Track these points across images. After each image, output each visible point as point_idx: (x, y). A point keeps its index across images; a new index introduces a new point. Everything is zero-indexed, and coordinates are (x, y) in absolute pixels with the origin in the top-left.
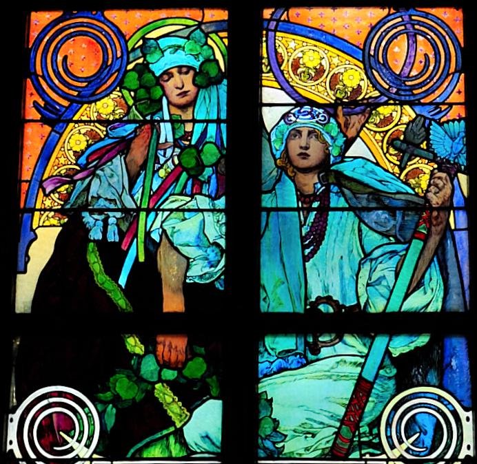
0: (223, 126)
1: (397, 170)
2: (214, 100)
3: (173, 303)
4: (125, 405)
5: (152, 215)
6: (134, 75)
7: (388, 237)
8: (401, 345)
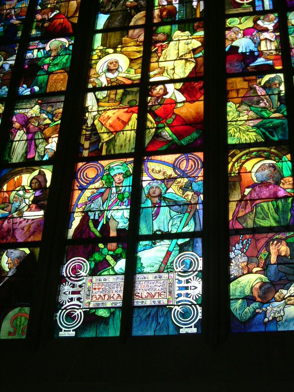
0: (131, 187)
1: (182, 195)
2: (128, 181)
3: (113, 234)
4: (97, 261)
5: (109, 211)
6: (106, 176)
7: (178, 213)
8: (181, 241)
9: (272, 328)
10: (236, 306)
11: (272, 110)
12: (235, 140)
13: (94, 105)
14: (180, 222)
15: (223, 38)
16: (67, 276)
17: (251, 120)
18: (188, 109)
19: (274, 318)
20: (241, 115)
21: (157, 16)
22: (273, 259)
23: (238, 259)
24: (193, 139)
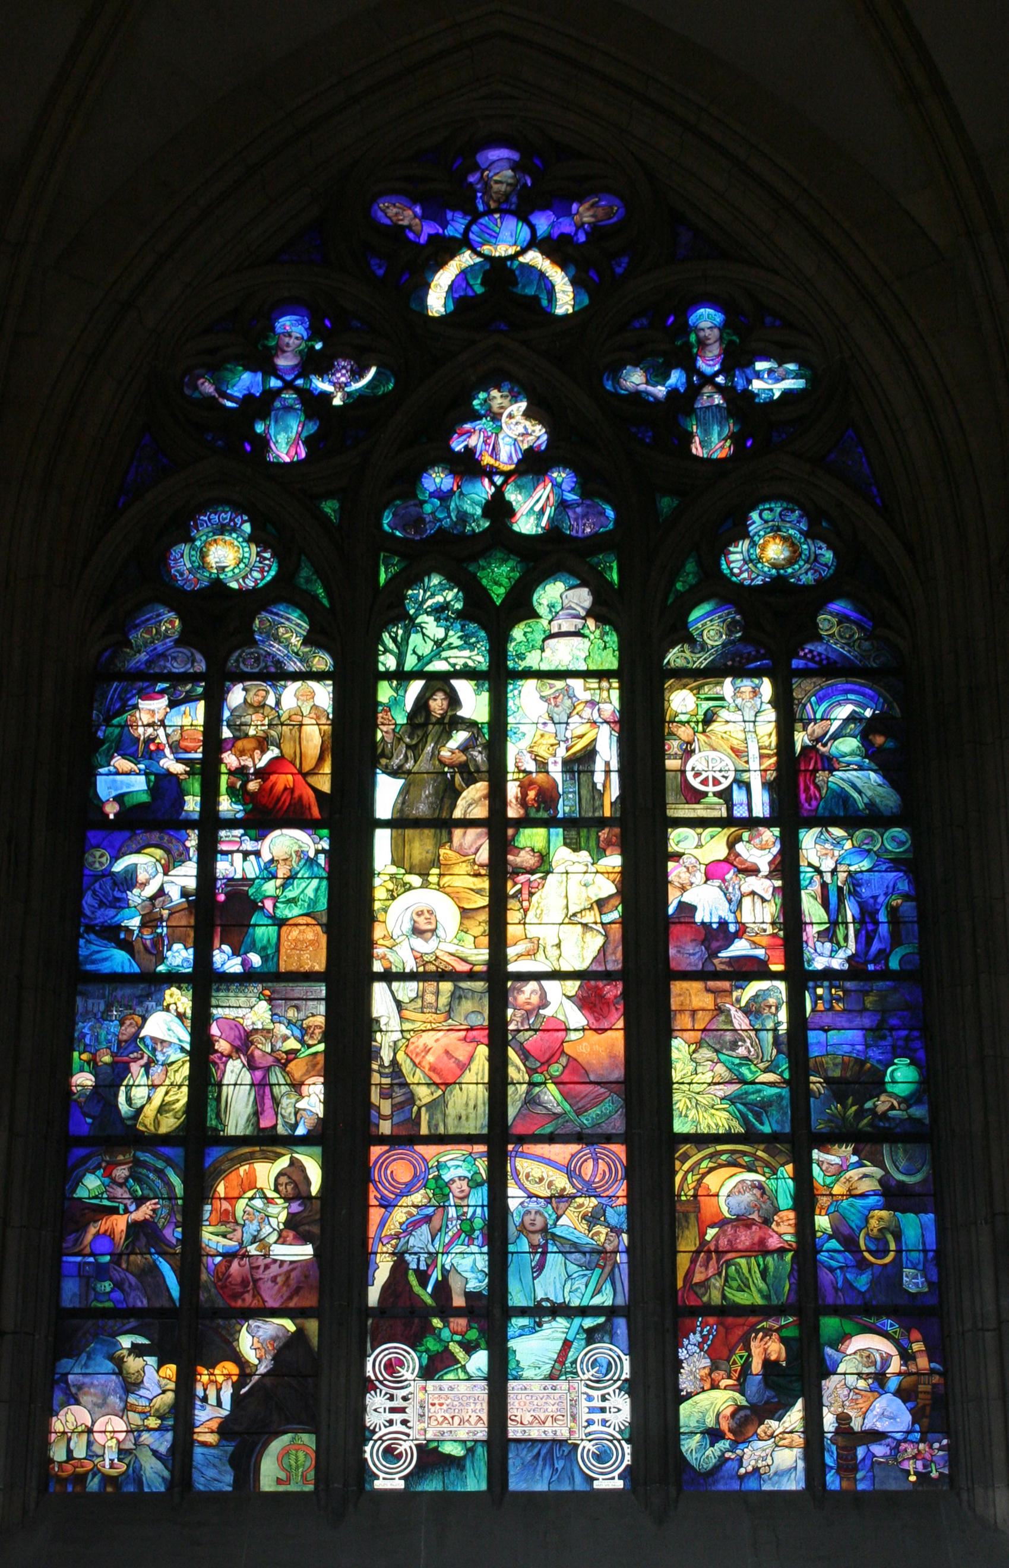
0: (486, 1209)
3: (459, 1301)
6: (433, 1181)
8: (589, 1323)
9: (752, 1485)
10: (690, 1445)
11: (762, 1066)
12: (689, 1123)
13: (392, 1015)
14: (586, 1287)
15: (662, 881)
16: (377, 1379)
17: (719, 1083)
18: (592, 1045)
19: (756, 1469)
20: (700, 1069)
21: (514, 801)
22: (756, 1366)
23: (693, 1363)
24: (605, 1114)
